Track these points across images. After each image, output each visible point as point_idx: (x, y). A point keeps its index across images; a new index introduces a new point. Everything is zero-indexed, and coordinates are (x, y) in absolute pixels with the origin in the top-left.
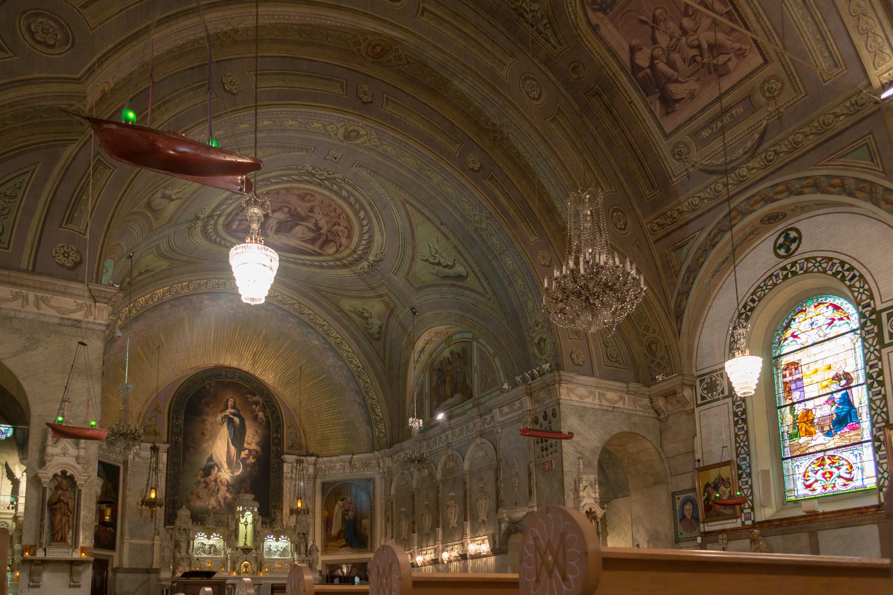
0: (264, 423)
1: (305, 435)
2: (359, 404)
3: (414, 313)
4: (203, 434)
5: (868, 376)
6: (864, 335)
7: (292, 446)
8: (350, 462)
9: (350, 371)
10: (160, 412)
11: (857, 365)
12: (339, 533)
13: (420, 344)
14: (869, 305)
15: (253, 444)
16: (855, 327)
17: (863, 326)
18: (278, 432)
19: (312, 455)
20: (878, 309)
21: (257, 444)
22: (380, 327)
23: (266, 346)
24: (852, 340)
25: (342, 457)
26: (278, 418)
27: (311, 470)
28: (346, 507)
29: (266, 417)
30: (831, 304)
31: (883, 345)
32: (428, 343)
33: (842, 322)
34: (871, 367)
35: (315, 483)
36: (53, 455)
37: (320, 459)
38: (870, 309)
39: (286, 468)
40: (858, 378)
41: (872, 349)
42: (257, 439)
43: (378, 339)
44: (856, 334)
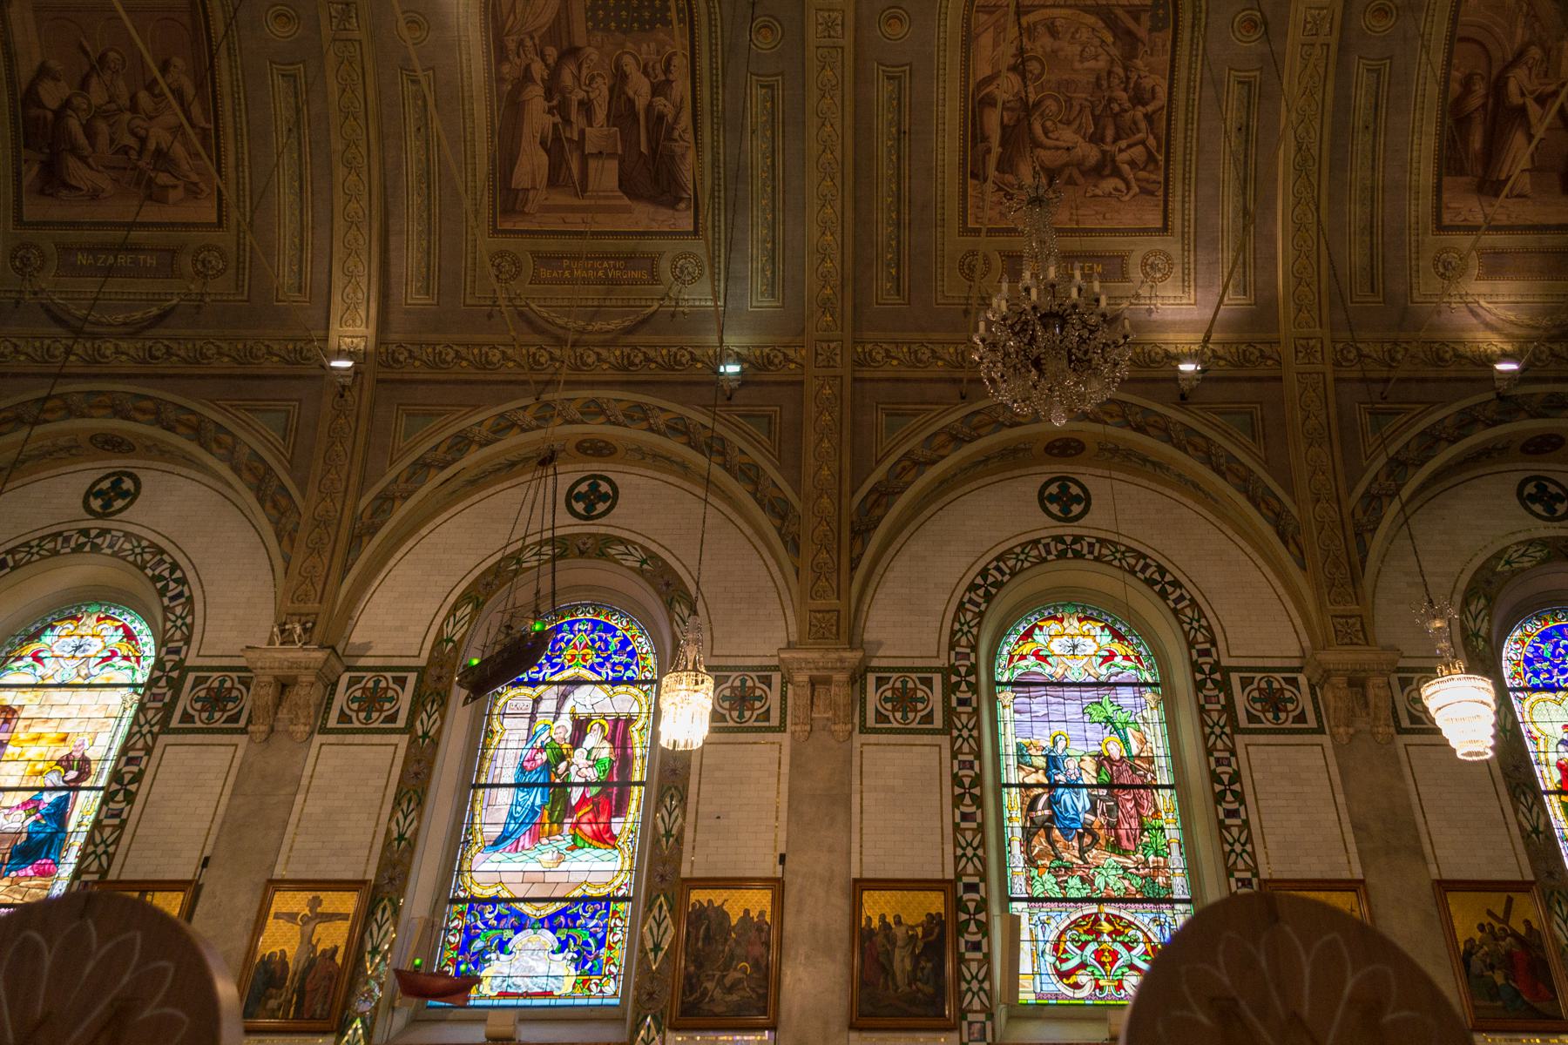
5: (116, 776)
6: (145, 700)
11: (110, 749)
14: (177, 651)
16: (140, 681)
17: (152, 682)
20: (188, 663)
24: (125, 701)
30: (124, 626)
31: (165, 729)
33: (126, 664)
34: (130, 761)
38: (176, 658)
40: (99, 774)
41: (145, 729)
44: (136, 692)
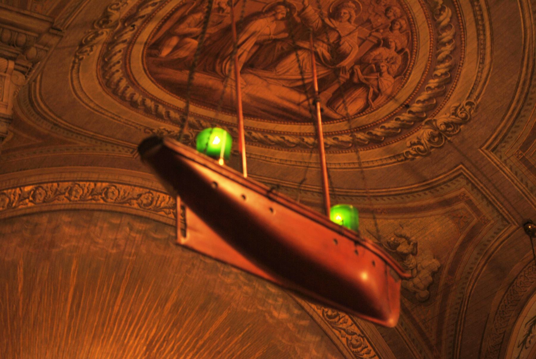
22: (434, 274)
43: (426, 301)
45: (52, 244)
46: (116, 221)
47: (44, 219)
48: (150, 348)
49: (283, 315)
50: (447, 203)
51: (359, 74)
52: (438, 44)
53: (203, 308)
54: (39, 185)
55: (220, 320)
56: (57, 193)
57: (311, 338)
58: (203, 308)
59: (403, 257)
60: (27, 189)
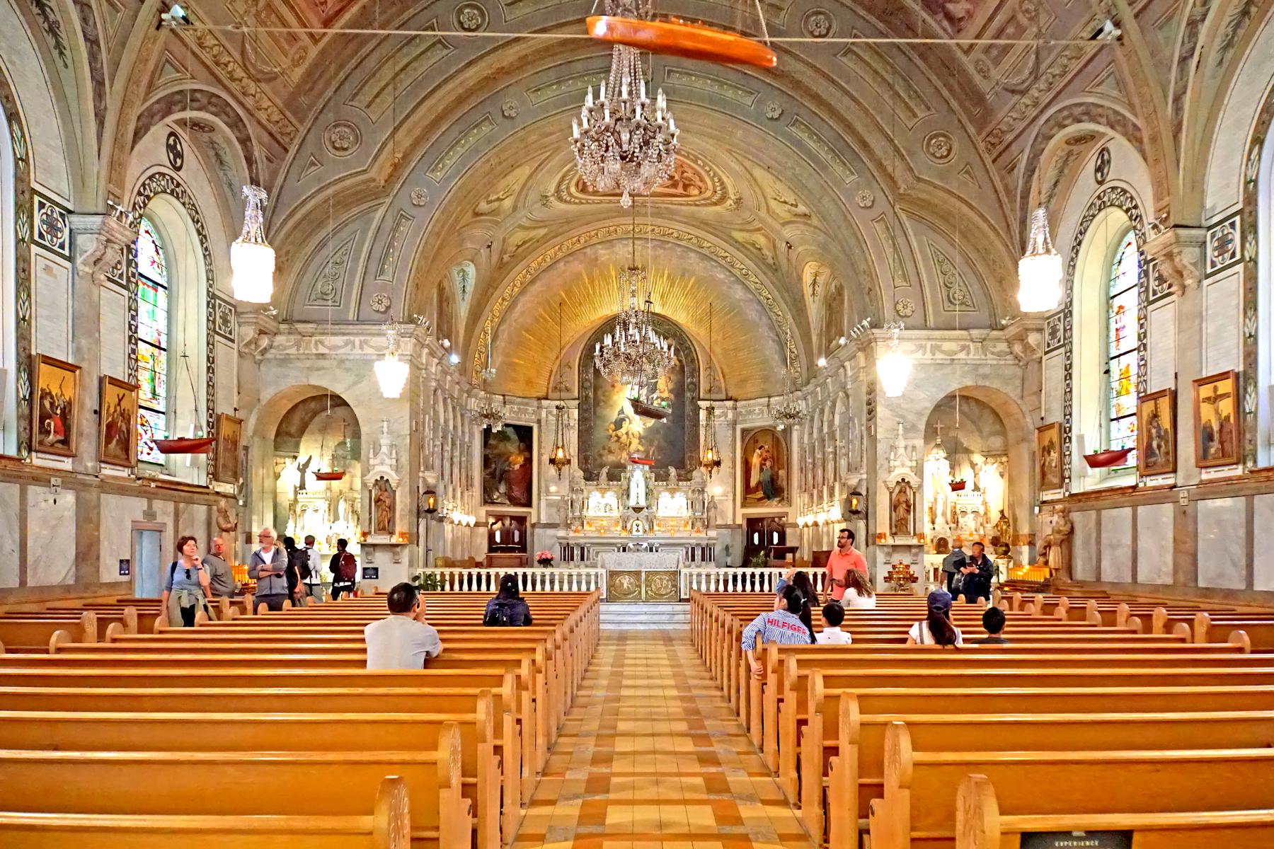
0: (677, 368)
1: (724, 377)
2: (774, 341)
3: (790, 247)
4: (613, 386)
7: (710, 391)
8: (768, 405)
9: (759, 302)
10: (570, 367)
12: (759, 483)
13: (807, 278)
15: (666, 392)
18: (693, 377)
19: (730, 399)
21: (670, 391)
23: (672, 285)
25: (759, 400)
26: (693, 360)
27: (730, 415)
28: (764, 454)
29: (680, 361)
32: (816, 276)
35: (734, 429)
36: (374, 466)
37: (739, 404)
39: (703, 414)
42: (671, 386)
45: (596, 259)
46: (625, 242)
47: (588, 250)
48: (662, 297)
49: (722, 276)
50: (759, 230)
51: (687, 182)
52: (707, 172)
53: (683, 275)
54: (580, 236)
55: (692, 280)
56: (591, 237)
57: (739, 287)
58: (683, 275)
59: (760, 249)
60: (575, 239)
